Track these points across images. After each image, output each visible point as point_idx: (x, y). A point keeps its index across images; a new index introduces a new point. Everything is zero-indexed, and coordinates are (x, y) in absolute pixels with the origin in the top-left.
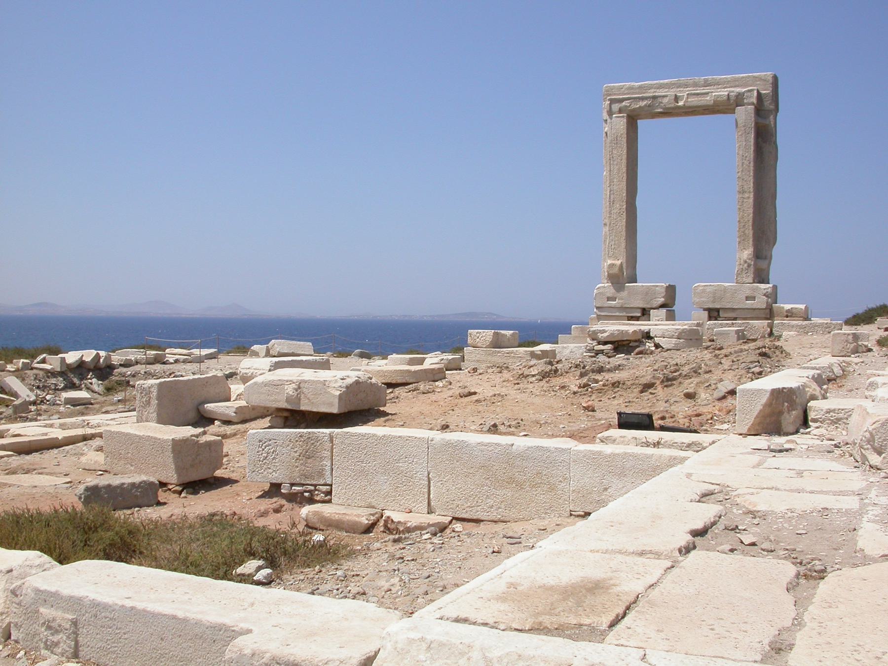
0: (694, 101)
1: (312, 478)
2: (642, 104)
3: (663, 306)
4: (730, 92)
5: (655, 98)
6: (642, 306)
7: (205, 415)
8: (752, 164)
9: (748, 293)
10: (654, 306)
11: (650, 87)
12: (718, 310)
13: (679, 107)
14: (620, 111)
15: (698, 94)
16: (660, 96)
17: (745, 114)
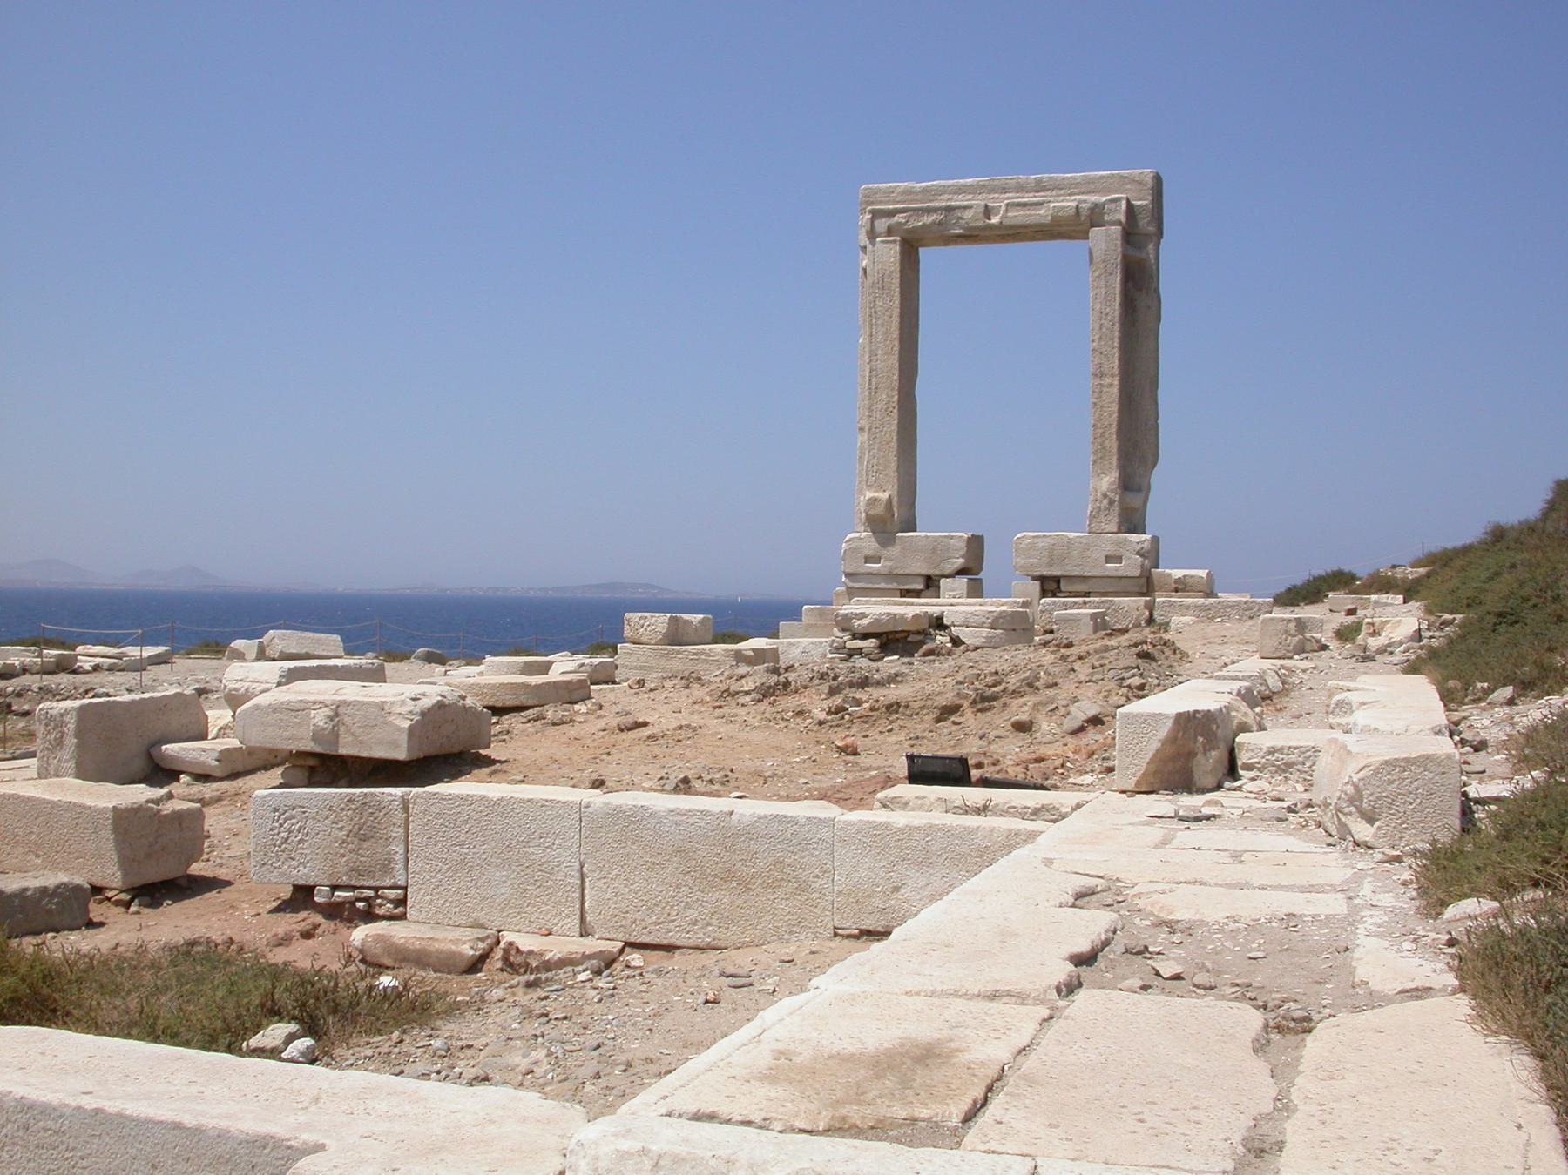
0: (1018, 217)
1: (369, 874)
2: (929, 219)
3: (962, 572)
4: (1080, 202)
5: (949, 209)
6: (924, 571)
7: (162, 764)
8: (1117, 327)
9: (1110, 549)
10: (947, 572)
11: (942, 191)
12: (1057, 580)
13: (992, 227)
14: (889, 232)
15: (1024, 205)
16: (959, 208)
17: (1105, 241)
